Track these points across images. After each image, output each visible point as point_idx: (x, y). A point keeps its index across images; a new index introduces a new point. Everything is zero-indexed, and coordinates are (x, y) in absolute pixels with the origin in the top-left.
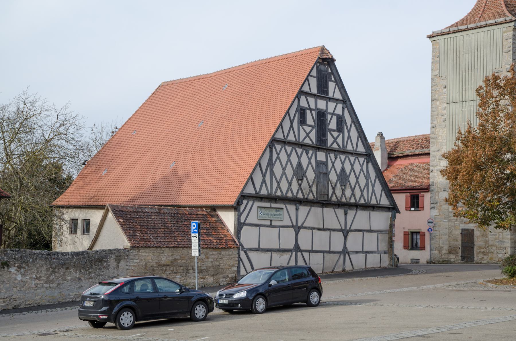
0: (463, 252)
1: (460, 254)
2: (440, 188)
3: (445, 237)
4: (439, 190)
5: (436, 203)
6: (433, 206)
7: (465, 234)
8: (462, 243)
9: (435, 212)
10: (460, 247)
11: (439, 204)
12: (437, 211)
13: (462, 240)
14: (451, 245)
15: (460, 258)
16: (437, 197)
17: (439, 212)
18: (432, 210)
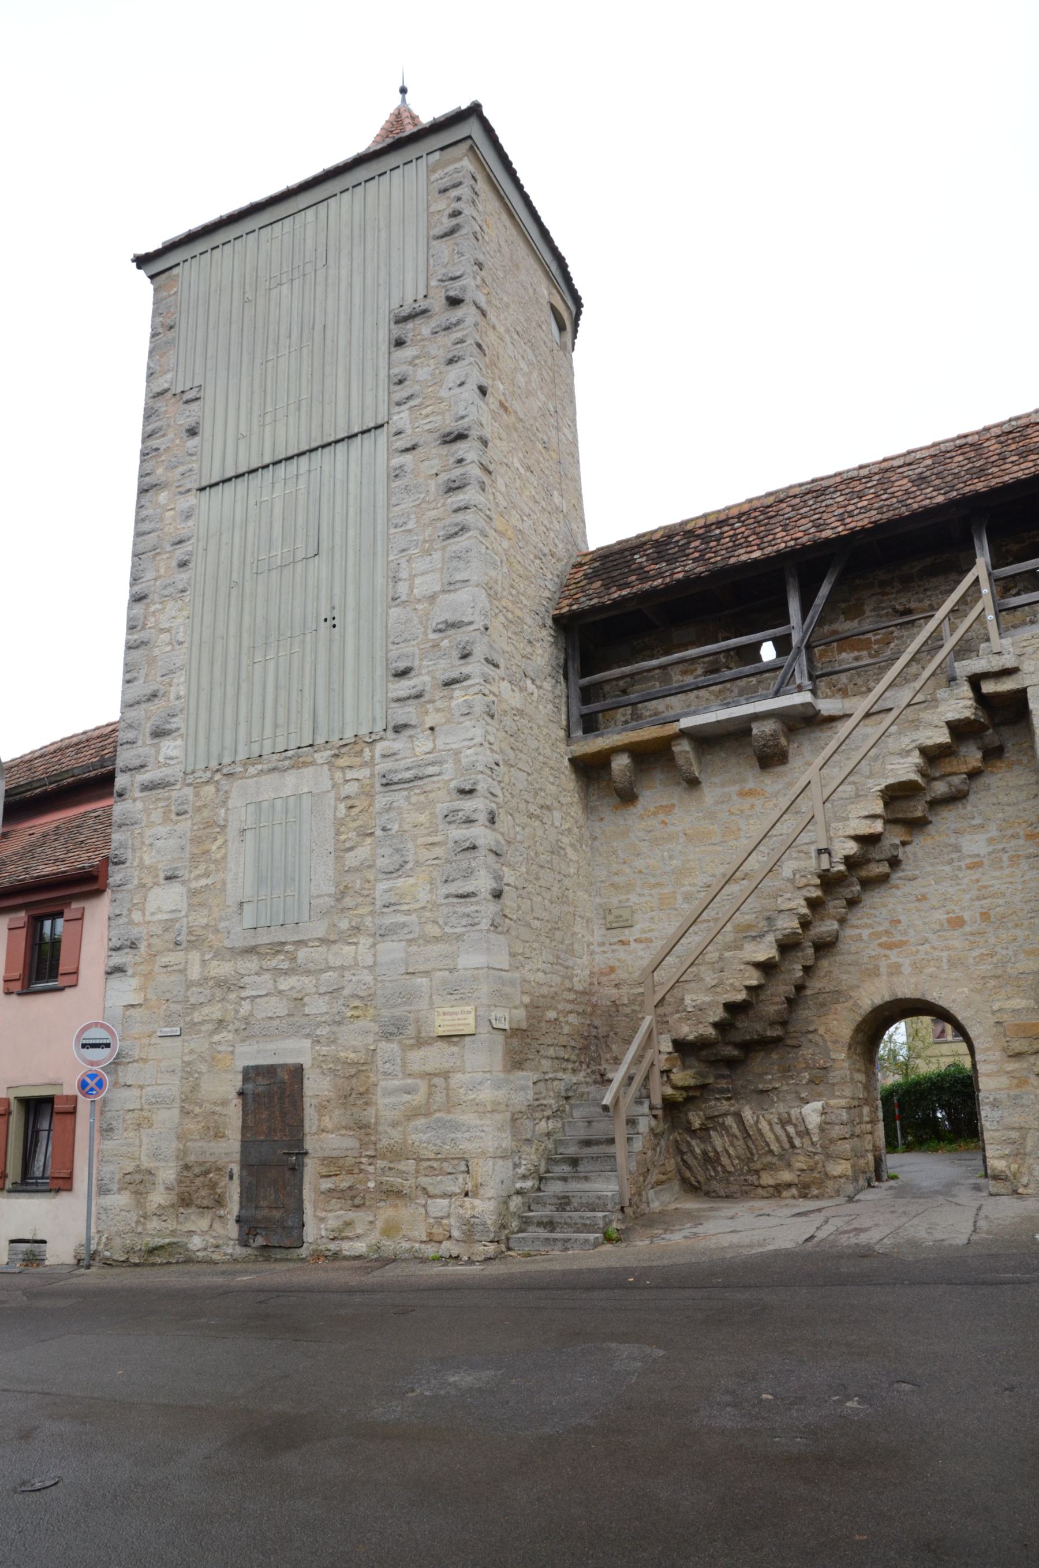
0: (248, 1196)
1: (233, 1207)
2: (152, 869)
3: (167, 1117)
4: (148, 880)
5: (133, 946)
6: (117, 959)
7: (256, 1096)
8: (244, 1143)
9: (124, 991)
10: (236, 1169)
11: (143, 947)
12: (135, 982)
13: (245, 1128)
14: (191, 1159)
15: (233, 1230)
16: (136, 916)
17: (143, 988)
18: (115, 982)
